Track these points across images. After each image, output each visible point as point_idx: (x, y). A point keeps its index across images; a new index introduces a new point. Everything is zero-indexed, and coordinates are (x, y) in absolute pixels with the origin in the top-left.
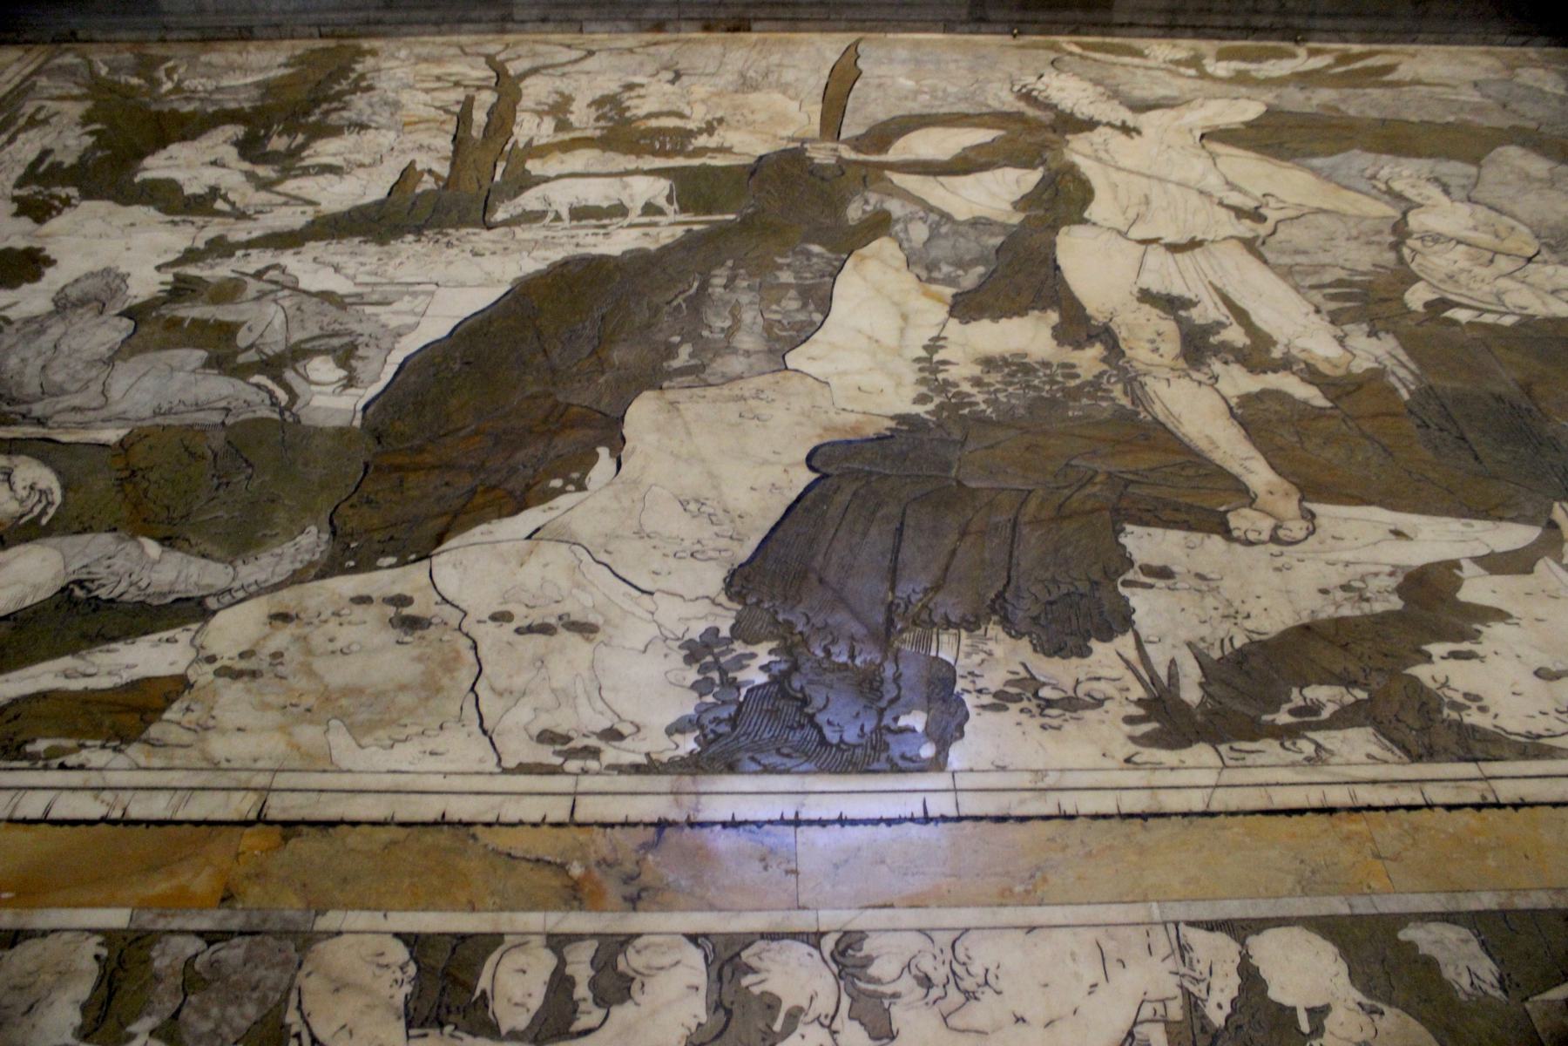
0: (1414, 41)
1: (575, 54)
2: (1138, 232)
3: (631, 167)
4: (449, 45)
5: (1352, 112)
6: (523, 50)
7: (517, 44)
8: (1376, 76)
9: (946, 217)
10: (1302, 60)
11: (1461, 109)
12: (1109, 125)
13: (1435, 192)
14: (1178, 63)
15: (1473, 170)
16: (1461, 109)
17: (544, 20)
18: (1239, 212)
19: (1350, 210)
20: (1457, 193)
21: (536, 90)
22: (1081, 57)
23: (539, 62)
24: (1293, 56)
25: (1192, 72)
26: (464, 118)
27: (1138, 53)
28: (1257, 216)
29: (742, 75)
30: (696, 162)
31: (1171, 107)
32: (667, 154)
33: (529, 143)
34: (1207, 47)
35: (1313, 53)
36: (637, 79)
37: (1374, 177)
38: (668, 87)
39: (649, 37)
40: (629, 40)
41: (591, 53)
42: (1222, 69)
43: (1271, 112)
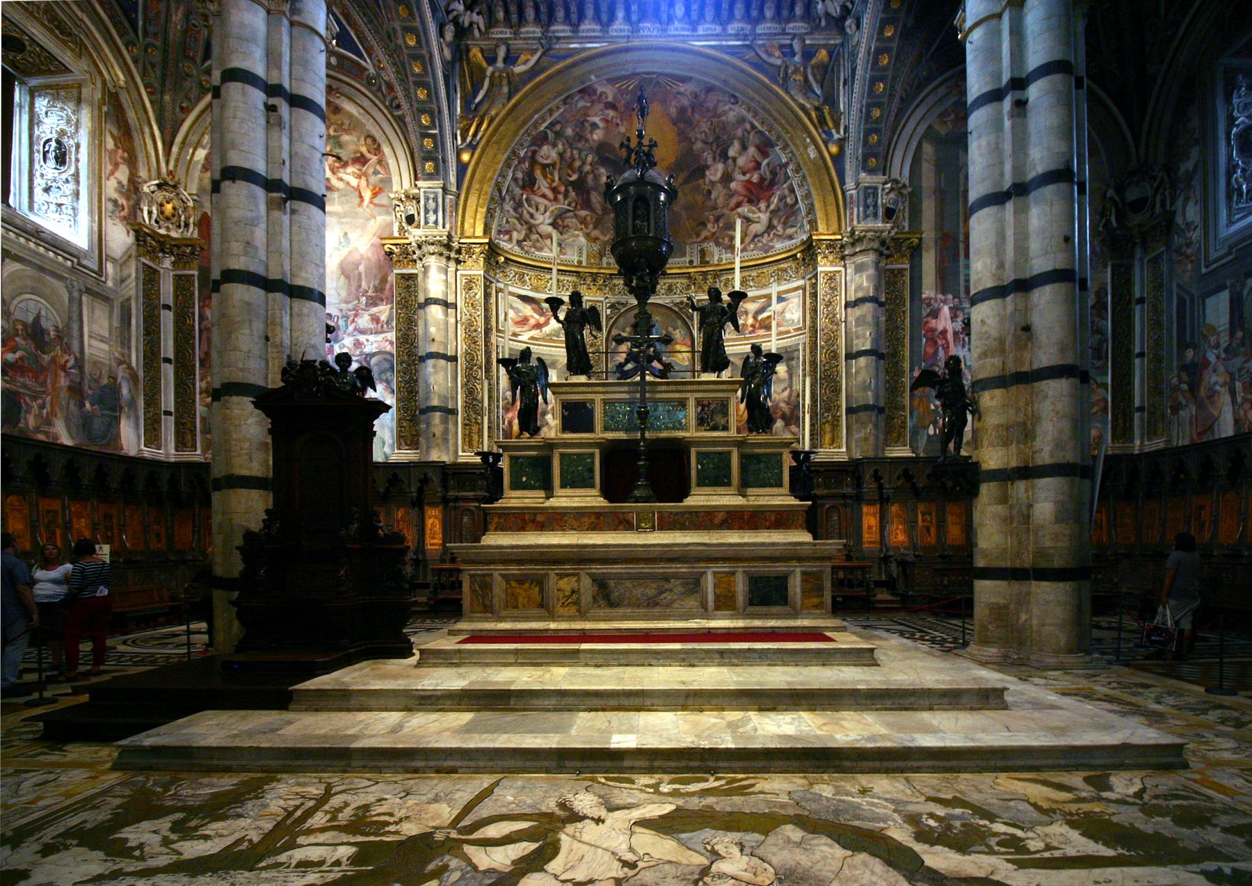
0: (769, 772)
1: (371, 783)
2: (563, 877)
3: (345, 841)
4: (315, 777)
5: (718, 809)
6: (346, 781)
7: (347, 778)
8: (742, 791)
9: (475, 868)
10: (712, 783)
11: (775, 806)
12: (592, 819)
13: (735, 850)
14: (647, 786)
15: (763, 837)
16: (775, 806)
17: (364, 767)
18: (626, 864)
19: (685, 861)
20: (747, 850)
21: (336, 801)
22: (603, 784)
23: (352, 786)
24: (707, 780)
25: (652, 790)
26: (290, 814)
27: (632, 782)
28: (633, 866)
29: (437, 795)
30: (378, 839)
31: (628, 808)
32: (367, 835)
33: (308, 828)
34: (666, 777)
35: (717, 779)
36: (386, 797)
37: (708, 843)
38: (398, 800)
39: (409, 776)
40: (400, 777)
41: (377, 783)
42: (665, 788)
43: (678, 809)
